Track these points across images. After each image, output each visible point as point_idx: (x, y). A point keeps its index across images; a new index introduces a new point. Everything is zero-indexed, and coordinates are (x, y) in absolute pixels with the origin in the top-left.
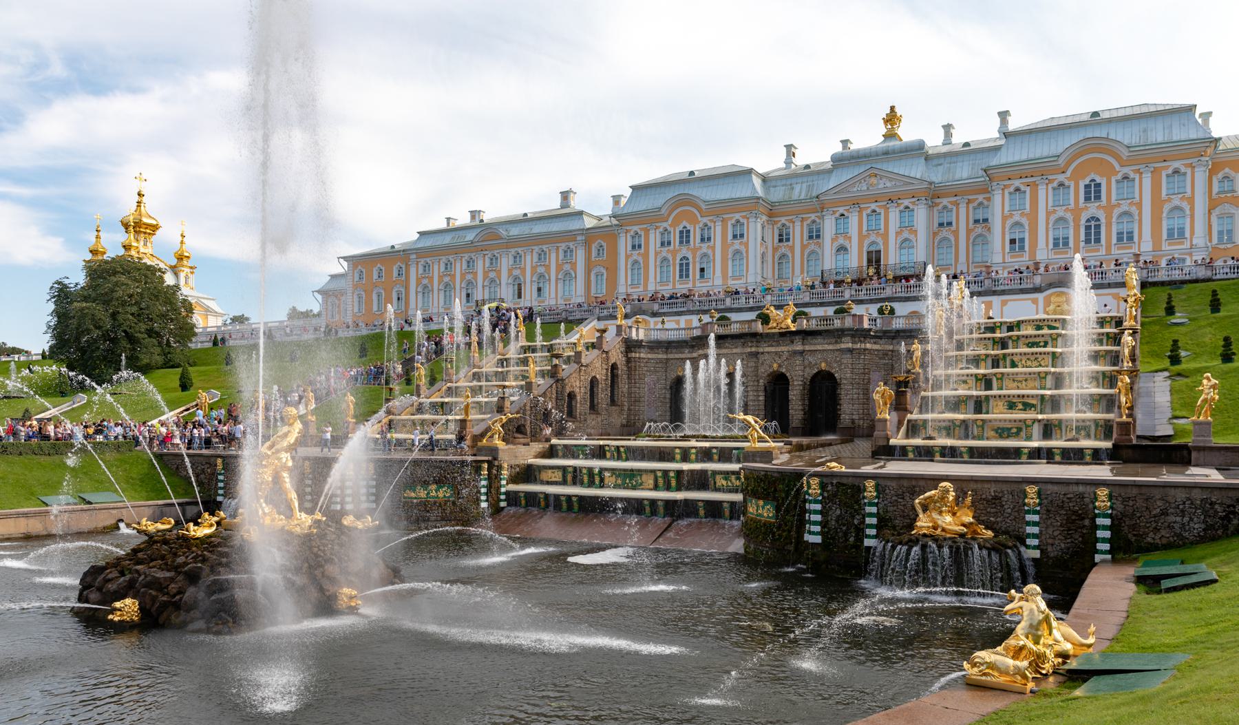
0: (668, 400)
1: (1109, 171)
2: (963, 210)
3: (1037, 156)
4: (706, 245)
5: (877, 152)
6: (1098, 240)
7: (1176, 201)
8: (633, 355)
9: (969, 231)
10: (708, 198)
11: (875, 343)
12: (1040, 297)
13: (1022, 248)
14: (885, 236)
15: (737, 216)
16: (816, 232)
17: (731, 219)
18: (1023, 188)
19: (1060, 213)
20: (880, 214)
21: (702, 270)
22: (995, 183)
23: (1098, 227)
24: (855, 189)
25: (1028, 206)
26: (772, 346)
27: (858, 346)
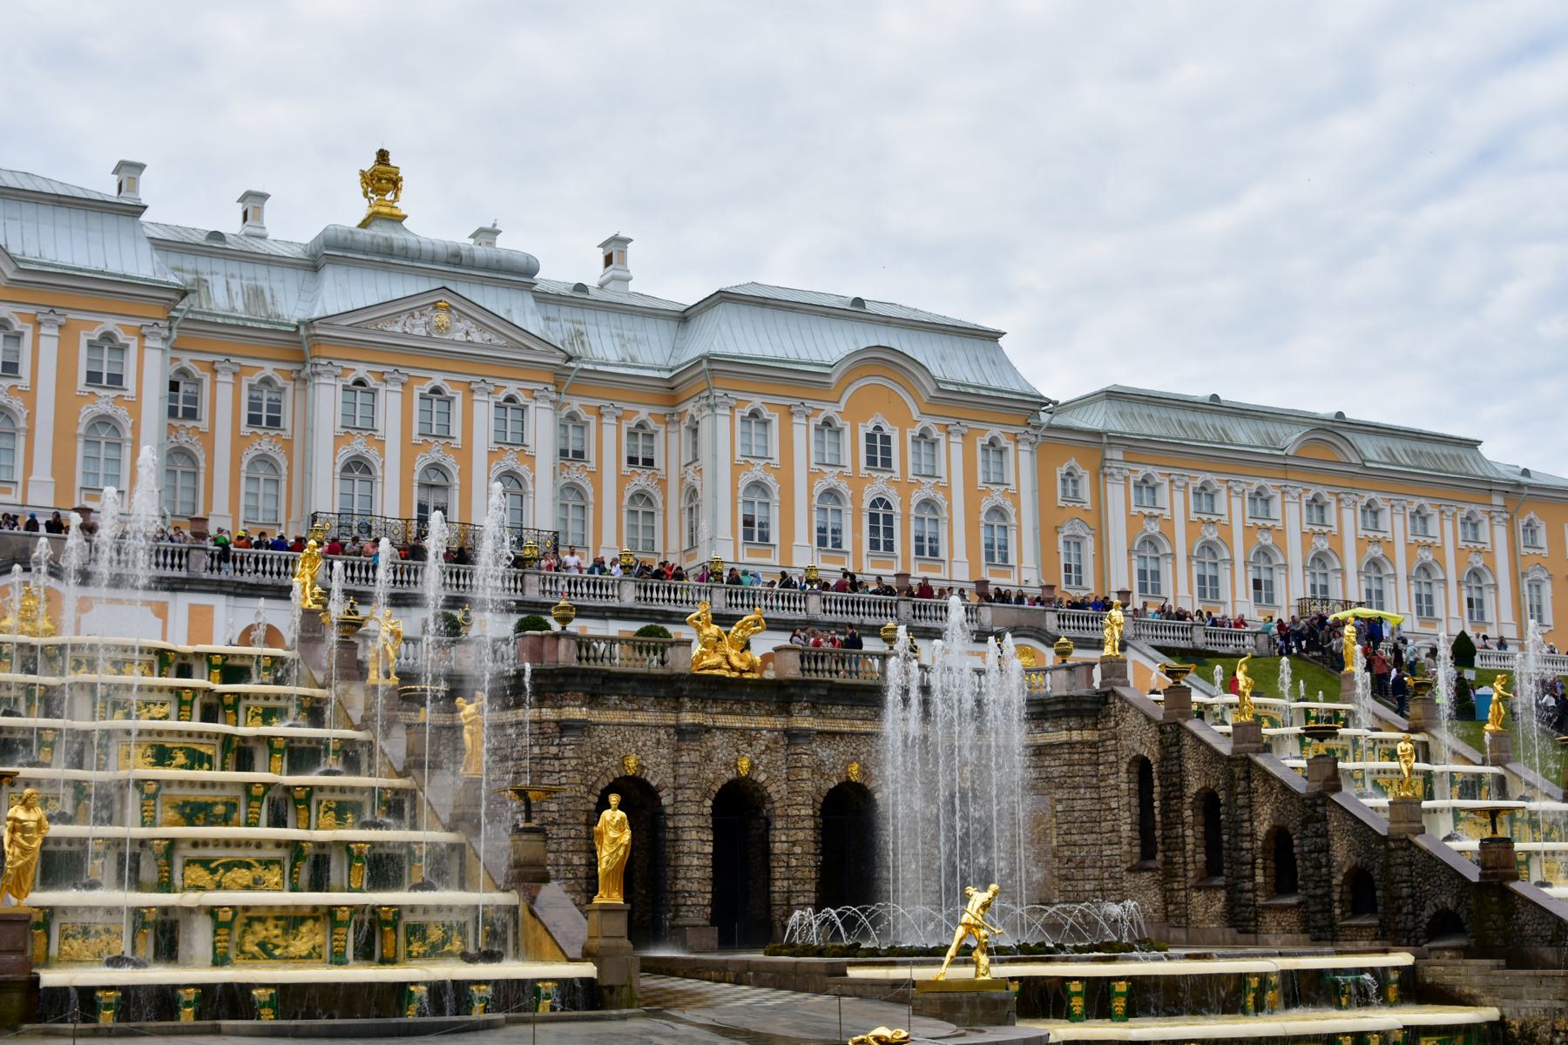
1: (905, 421)
2: (609, 432)
3: (792, 356)
5: (434, 253)
6: (889, 546)
7: (997, 497)
9: (622, 479)
10: (31, 253)
13: (764, 537)
14: (465, 454)
15: (110, 324)
16: (270, 409)
18: (766, 414)
19: (831, 479)
20: (449, 401)
22: (719, 393)
23: (889, 519)
24: (398, 329)
25: (775, 451)
26: (732, 713)
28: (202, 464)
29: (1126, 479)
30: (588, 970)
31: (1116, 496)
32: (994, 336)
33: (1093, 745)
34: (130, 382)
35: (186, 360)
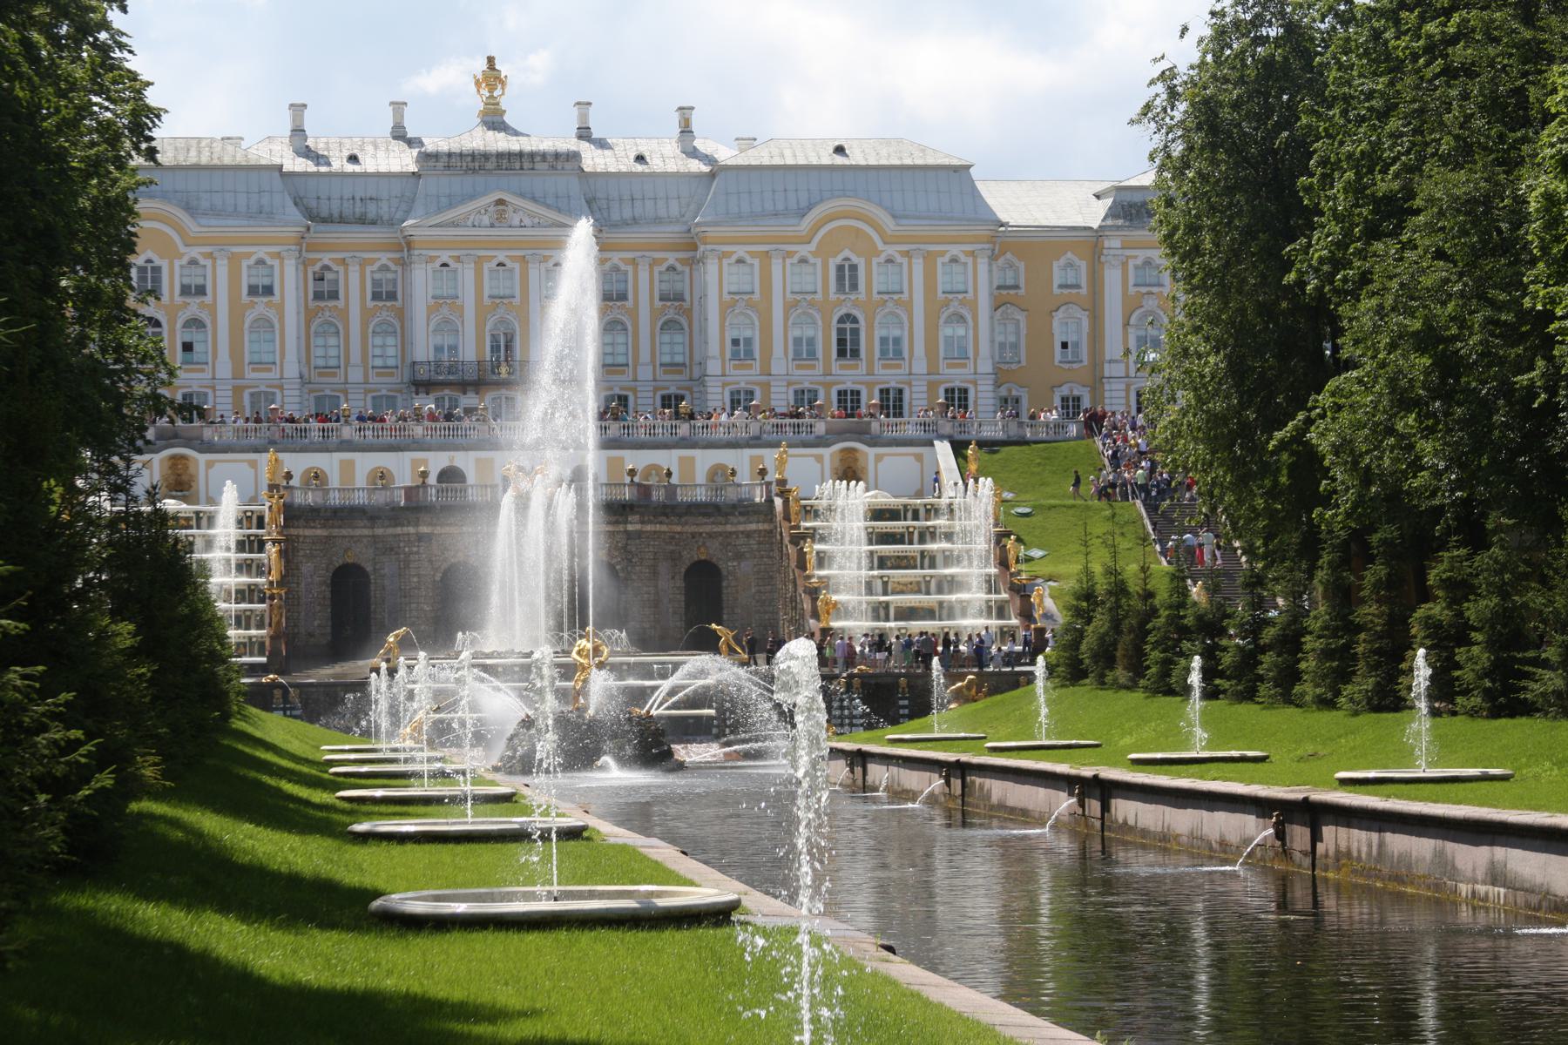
0: (328, 602)
2: (644, 275)
4: (198, 300)
6: (855, 353)
8: (293, 531)
11: (661, 523)
12: (826, 452)
13: (749, 354)
15: (261, 252)
17: (248, 255)
18: (749, 260)
20: (512, 270)
21: (188, 347)
23: (855, 332)
24: (469, 223)
25: (757, 290)
27: (649, 528)
28: (341, 331)
29: (1125, 265)
30: (264, 659)
31: (1112, 279)
32: (969, 167)
33: (771, 532)
34: (277, 290)
35: (326, 262)
